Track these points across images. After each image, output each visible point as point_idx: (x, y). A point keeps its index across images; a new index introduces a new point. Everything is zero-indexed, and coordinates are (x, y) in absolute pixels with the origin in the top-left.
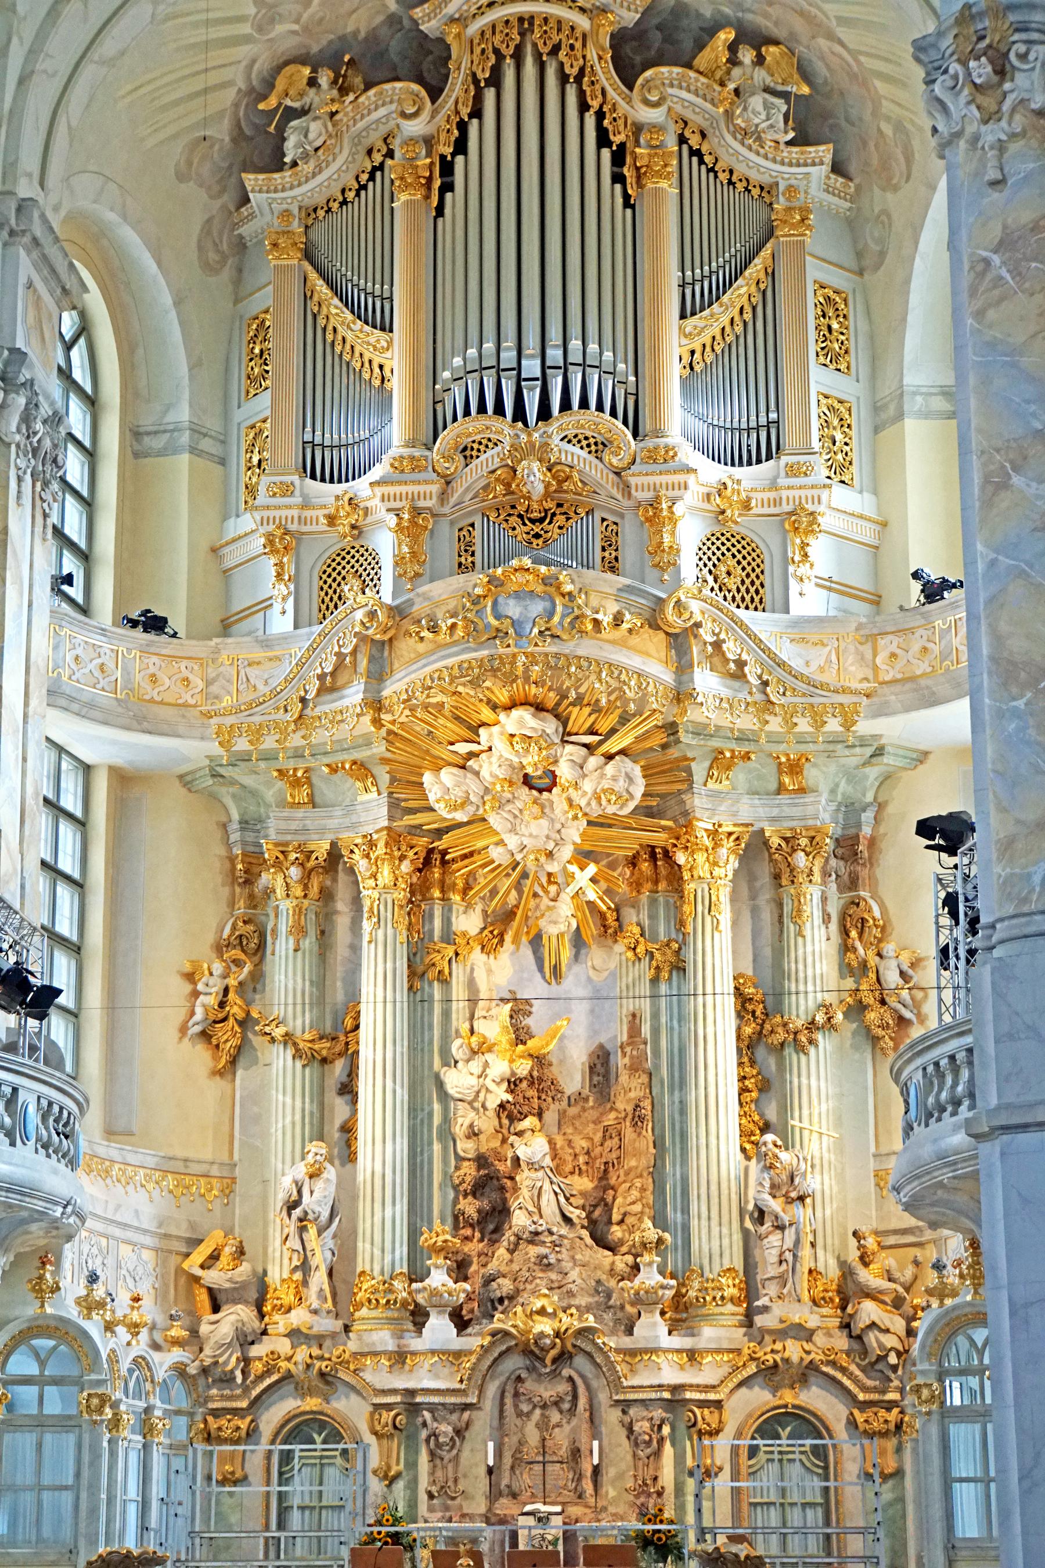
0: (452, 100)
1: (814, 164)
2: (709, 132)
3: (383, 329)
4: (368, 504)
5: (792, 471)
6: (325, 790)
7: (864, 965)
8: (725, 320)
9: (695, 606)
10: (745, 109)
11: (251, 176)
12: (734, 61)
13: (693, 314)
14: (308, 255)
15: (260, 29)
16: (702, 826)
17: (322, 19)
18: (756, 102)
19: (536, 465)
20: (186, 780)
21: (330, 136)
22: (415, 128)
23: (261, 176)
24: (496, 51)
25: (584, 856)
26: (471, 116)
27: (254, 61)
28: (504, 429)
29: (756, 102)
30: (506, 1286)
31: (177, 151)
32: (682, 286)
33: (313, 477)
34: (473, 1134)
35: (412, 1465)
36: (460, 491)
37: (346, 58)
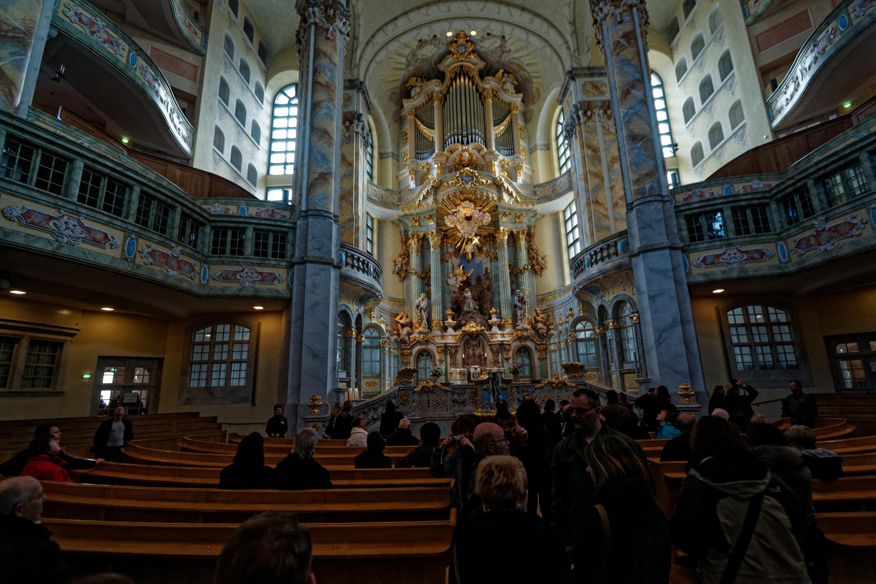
5: (517, 158)
6: (422, 223)
7: (533, 257)
12: (503, 76)
14: (416, 116)
16: (502, 228)
18: (509, 84)
20: (393, 222)
22: (437, 89)
25: (476, 235)
28: (460, 147)
29: (509, 84)
30: (464, 322)
31: (389, 94)
34: (454, 292)
35: (446, 358)
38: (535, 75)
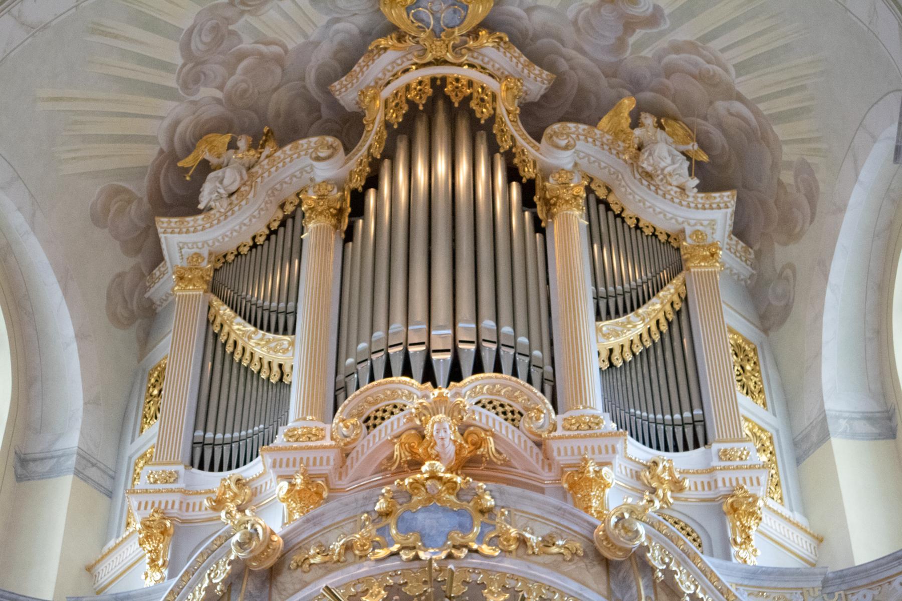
0: (364, 151)
1: (719, 208)
2: (614, 185)
3: (285, 332)
4: (257, 484)
8: (641, 328)
9: (641, 528)
10: (650, 154)
11: (165, 220)
12: (636, 123)
13: (609, 316)
14: (214, 288)
15: (185, 86)
17: (245, 91)
19: (448, 423)
21: (245, 184)
23: (174, 220)
24: (408, 101)
26: (385, 155)
27: (176, 123)
32: (597, 298)
33: (201, 467)
36: (362, 458)
37: (265, 130)
38: (782, 105)
